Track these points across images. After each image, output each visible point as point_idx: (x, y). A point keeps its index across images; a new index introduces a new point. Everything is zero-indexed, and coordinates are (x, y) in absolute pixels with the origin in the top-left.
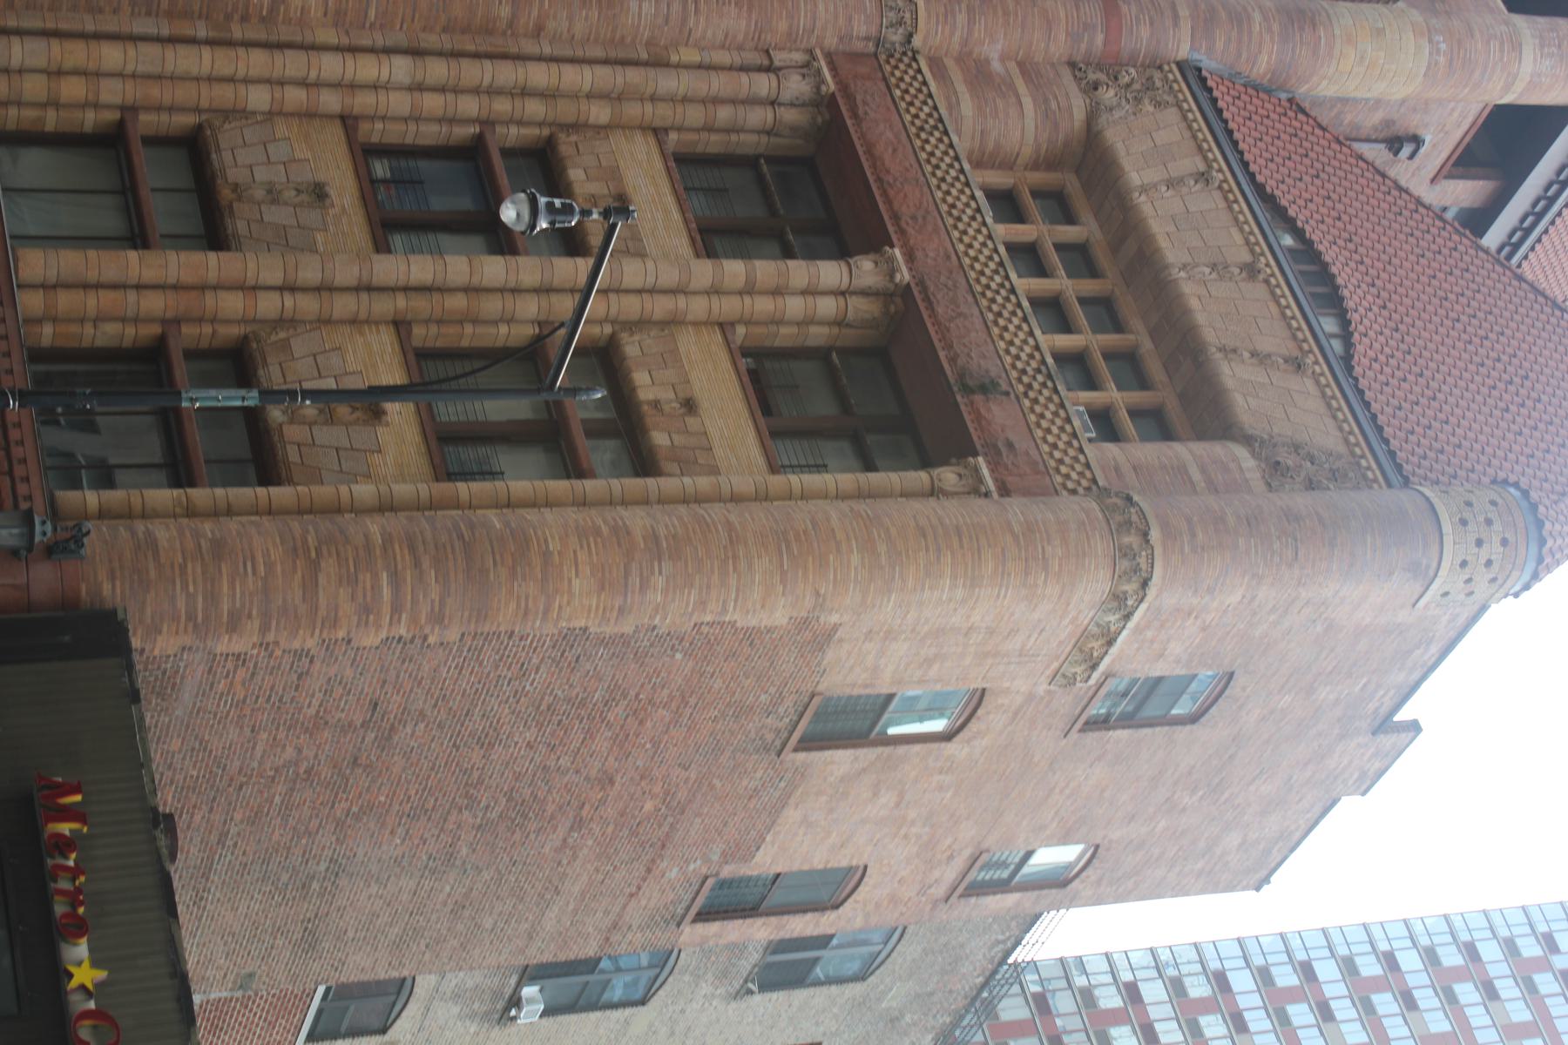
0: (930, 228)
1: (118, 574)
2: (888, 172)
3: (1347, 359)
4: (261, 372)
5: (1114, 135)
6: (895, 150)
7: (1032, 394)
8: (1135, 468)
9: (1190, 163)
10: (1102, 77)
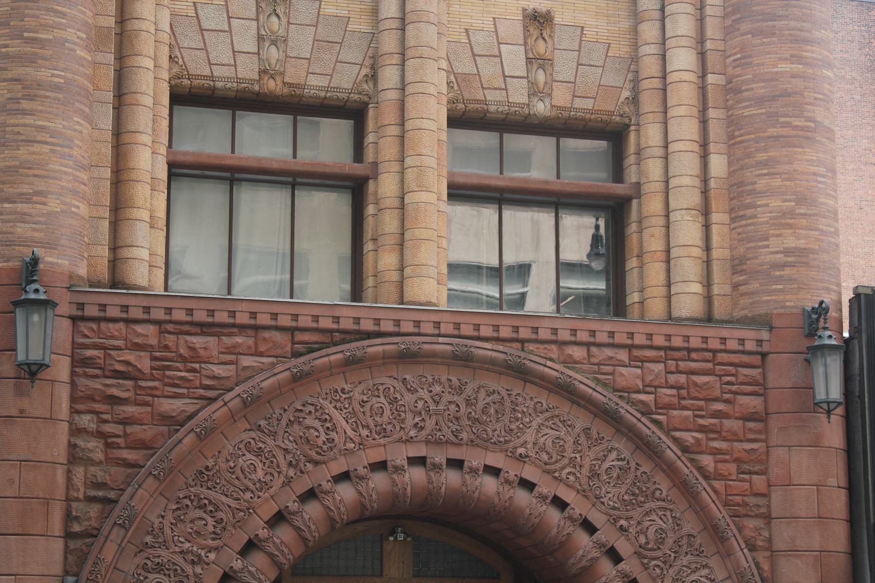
1: (827, 285)
4: (493, 108)
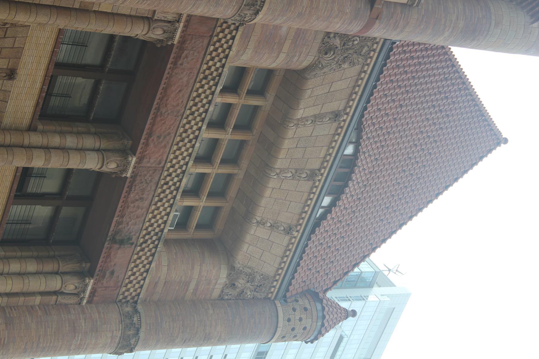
0: (163, 144)
2: (166, 106)
3: (317, 224)
5: (311, 84)
6: (180, 91)
7: (144, 246)
8: (165, 283)
9: (337, 105)
10: (337, 42)
